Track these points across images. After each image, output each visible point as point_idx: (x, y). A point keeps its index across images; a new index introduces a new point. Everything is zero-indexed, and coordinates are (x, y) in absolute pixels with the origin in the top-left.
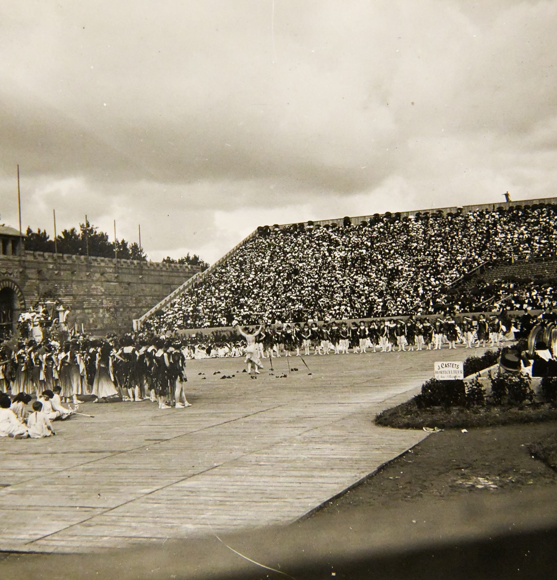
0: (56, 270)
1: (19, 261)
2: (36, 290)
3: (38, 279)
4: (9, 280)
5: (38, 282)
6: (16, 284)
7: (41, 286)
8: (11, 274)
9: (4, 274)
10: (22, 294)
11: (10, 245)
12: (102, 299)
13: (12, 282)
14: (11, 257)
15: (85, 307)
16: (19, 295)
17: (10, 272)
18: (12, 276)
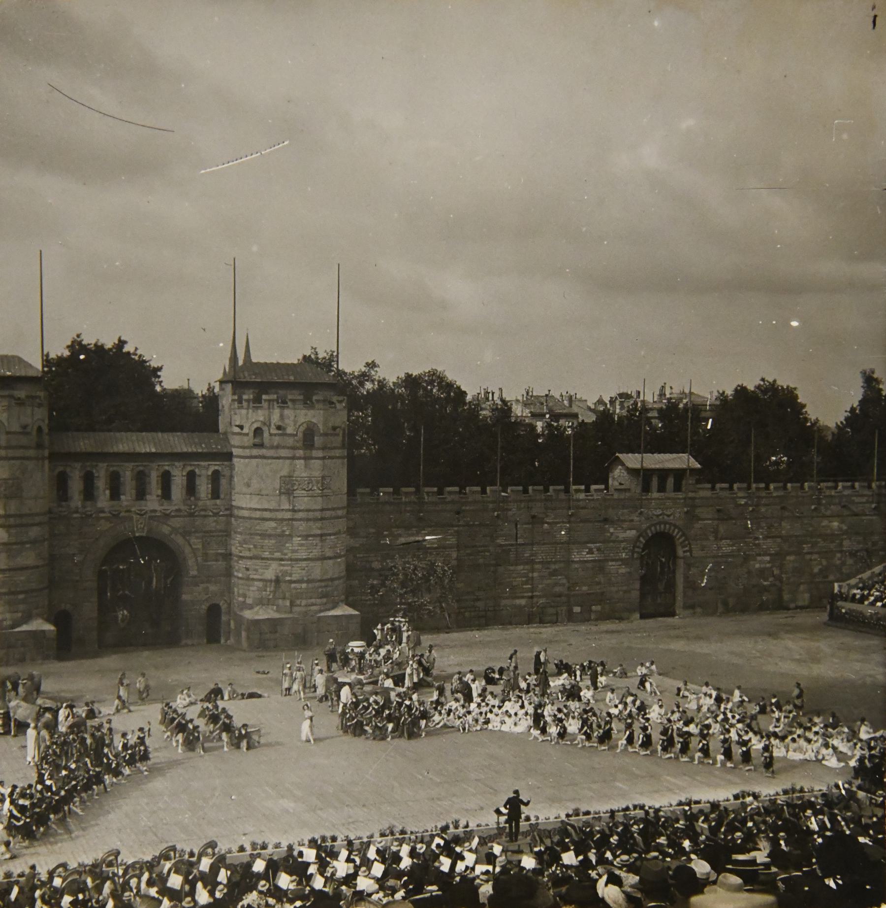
0: (751, 506)
1: (685, 499)
2: (713, 532)
3: (718, 519)
4: (665, 523)
5: (716, 522)
6: (676, 526)
7: (722, 529)
8: (668, 516)
9: (658, 516)
10: (687, 539)
11: (670, 482)
12: (842, 540)
13: (670, 524)
14: (672, 495)
15: (805, 551)
16: (681, 540)
17: (669, 513)
18: (672, 517)
